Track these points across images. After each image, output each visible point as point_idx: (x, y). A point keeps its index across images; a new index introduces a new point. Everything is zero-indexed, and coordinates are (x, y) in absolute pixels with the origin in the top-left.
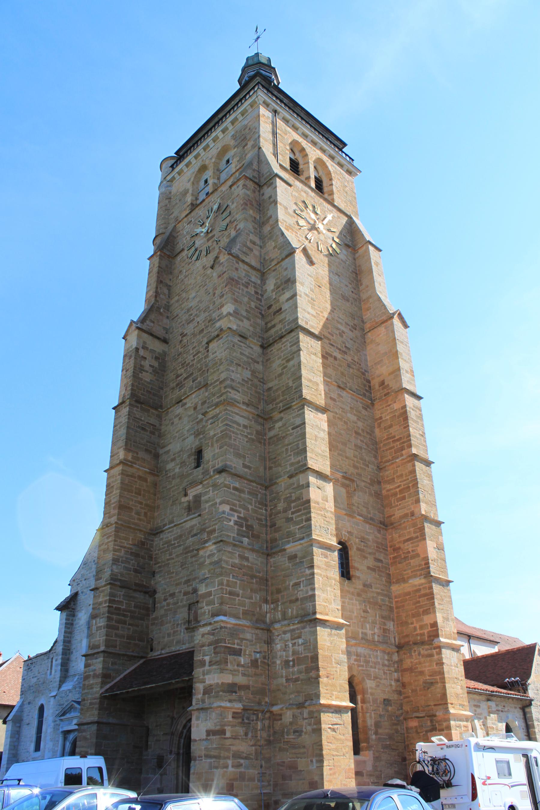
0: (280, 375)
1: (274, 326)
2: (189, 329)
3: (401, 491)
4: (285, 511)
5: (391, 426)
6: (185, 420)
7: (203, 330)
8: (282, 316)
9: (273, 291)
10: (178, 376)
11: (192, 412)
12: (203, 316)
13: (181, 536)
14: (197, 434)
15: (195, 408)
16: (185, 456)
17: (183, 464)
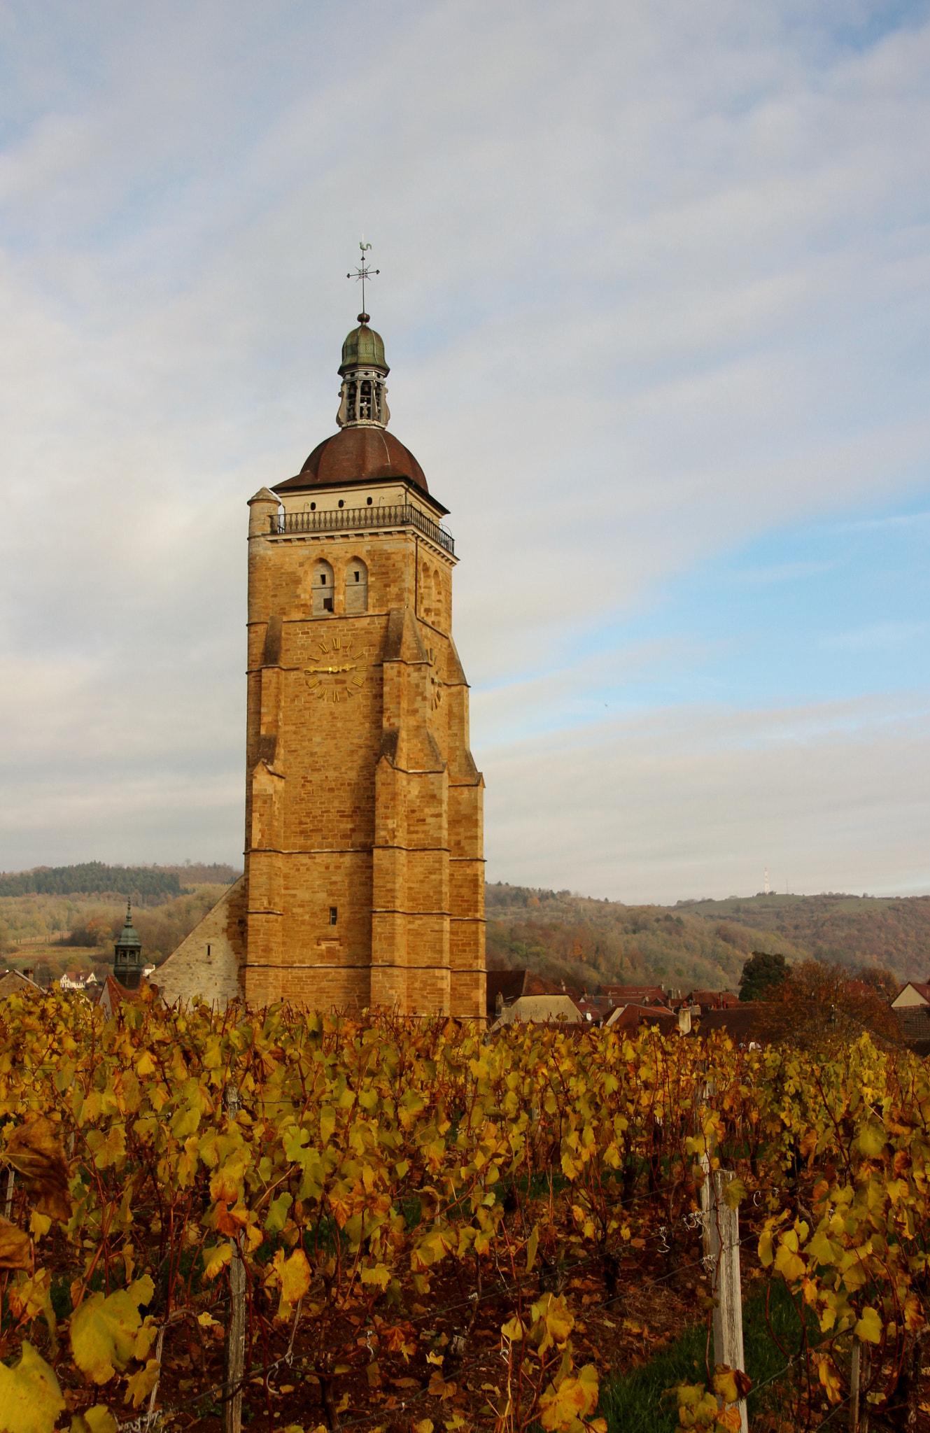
0: (422, 882)
1: (417, 832)
2: (315, 777)
3: (463, 945)
4: (421, 989)
5: (461, 887)
6: (315, 874)
7: (331, 790)
8: (426, 828)
9: (417, 797)
10: (301, 823)
11: (323, 869)
12: (332, 774)
13: (314, 977)
14: (331, 894)
15: (327, 868)
16: (317, 909)
17: (313, 914)
